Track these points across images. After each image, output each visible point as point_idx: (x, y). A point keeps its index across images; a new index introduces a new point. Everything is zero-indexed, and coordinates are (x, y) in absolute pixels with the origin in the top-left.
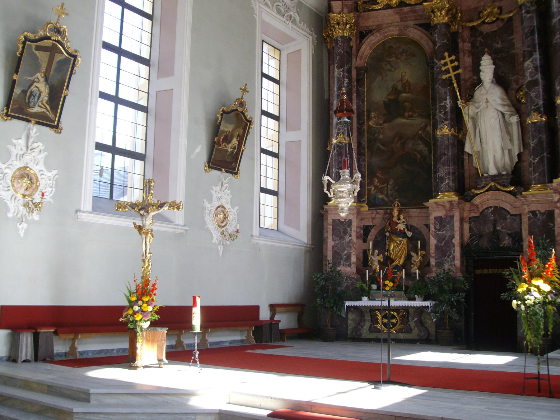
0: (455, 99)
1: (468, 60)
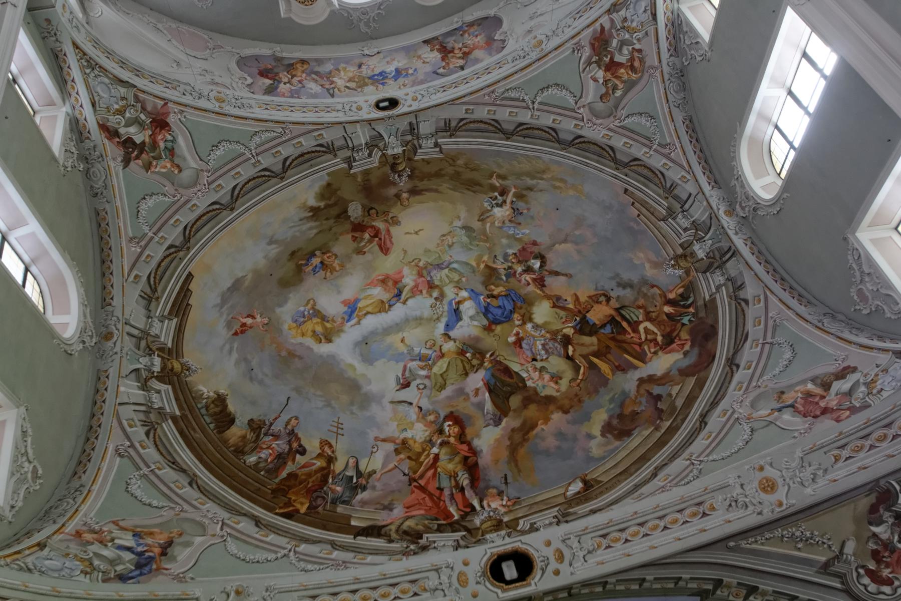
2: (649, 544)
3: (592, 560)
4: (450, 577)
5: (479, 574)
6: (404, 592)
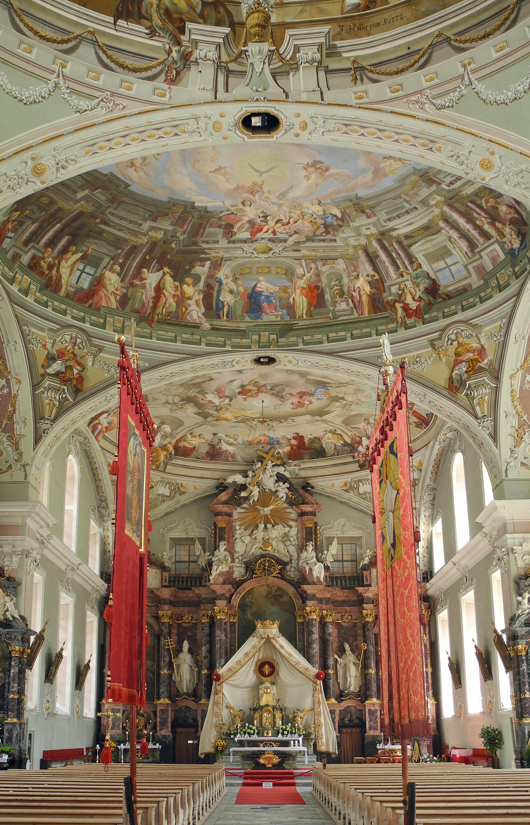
0: (171, 658)
1: (175, 638)
2: (378, 144)
3: (328, 136)
4: (207, 124)
5: (232, 124)
6: (166, 133)
